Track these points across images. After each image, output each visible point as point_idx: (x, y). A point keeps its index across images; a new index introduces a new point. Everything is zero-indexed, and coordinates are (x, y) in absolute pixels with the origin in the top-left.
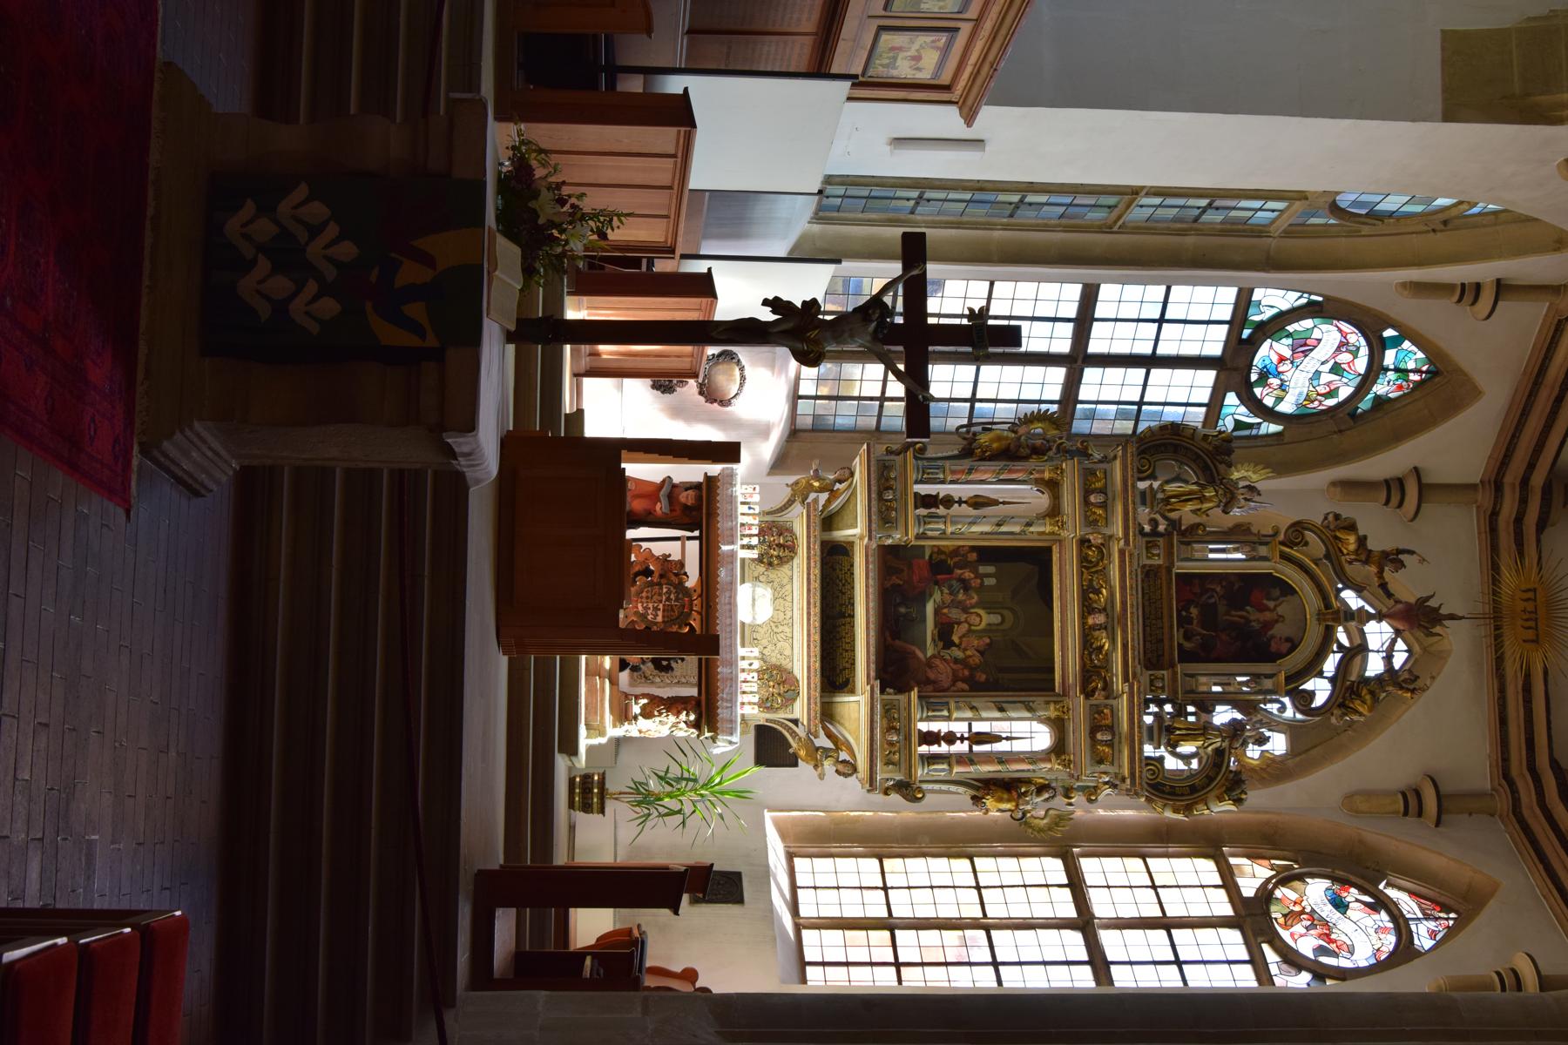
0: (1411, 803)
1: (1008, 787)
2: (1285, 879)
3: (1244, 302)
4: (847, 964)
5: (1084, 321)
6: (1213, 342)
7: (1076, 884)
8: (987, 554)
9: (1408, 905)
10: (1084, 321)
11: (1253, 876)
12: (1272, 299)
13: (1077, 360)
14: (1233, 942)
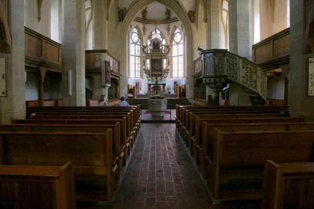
0: (169, 31)
1: (169, 62)
2: (174, 40)
3: (132, 43)
4: (178, 70)
5: (133, 56)
6: (134, 45)
7: (175, 56)
8: (152, 63)
9: (176, 32)
10: (133, 56)
11: (174, 43)
12: (131, 41)
13: (135, 56)
14: (179, 45)
